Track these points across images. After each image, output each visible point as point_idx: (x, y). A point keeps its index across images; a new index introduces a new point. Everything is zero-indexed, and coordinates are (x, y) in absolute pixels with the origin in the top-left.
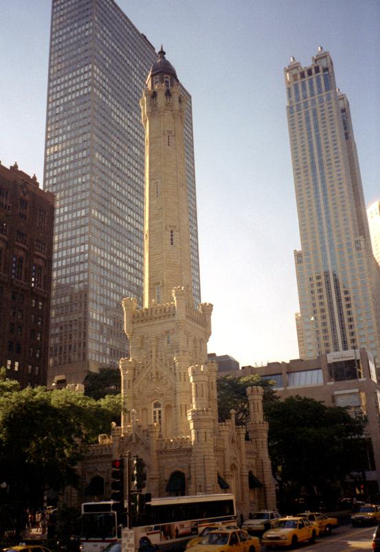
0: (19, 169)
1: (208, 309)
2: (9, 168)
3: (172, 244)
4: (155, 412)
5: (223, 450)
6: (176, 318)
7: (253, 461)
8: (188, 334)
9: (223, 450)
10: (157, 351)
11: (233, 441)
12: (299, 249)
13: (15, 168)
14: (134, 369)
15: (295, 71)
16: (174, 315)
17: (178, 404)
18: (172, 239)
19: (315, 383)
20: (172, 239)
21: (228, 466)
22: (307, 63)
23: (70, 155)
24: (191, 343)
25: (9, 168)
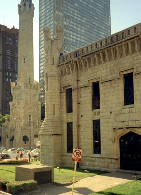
0: (15, 28)
2: (11, 29)
3: (25, 63)
4: (29, 118)
6: (21, 89)
10: (18, 100)
13: (13, 28)
18: (25, 61)
20: (25, 61)
23: (47, 13)
25: (11, 29)
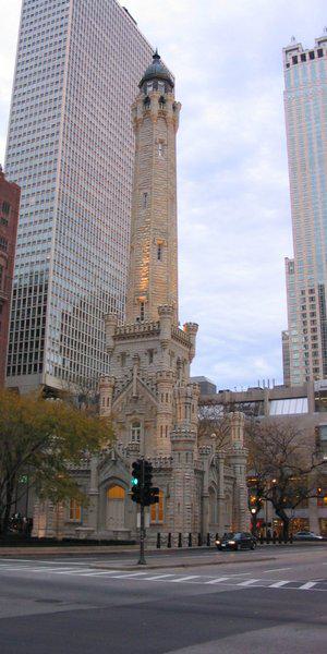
1: (192, 328)
5: (202, 473)
6: (161, 337)
7: (230, 487)
8: (172, 354)
9: (202, 473)
11: (212, 465)
12: (291, 257)
14: (114, 388)
15: (295, 53)
16: (158, 334)
17: (159, 425)
19: (299, 412)
21: (206, 488)
22: (309, 45)
24: (174, 364)
